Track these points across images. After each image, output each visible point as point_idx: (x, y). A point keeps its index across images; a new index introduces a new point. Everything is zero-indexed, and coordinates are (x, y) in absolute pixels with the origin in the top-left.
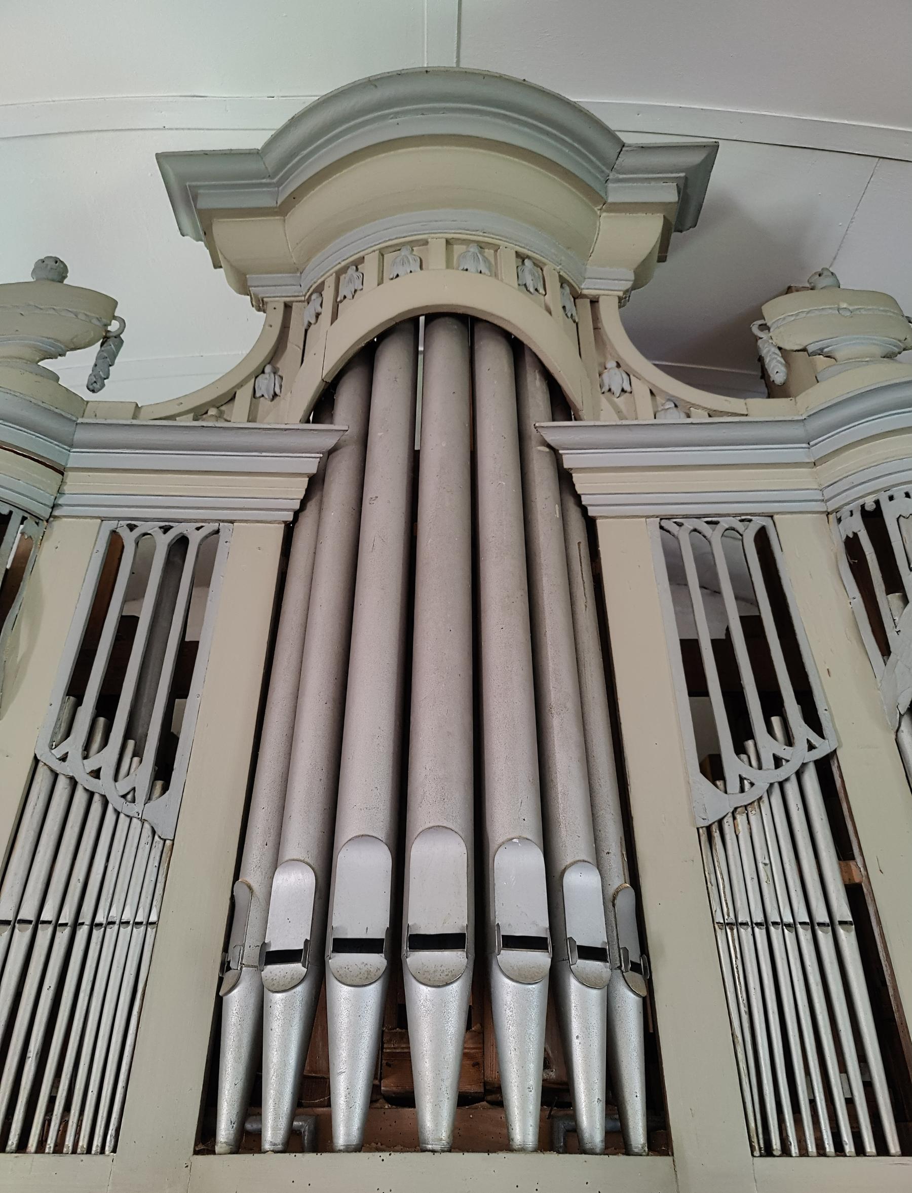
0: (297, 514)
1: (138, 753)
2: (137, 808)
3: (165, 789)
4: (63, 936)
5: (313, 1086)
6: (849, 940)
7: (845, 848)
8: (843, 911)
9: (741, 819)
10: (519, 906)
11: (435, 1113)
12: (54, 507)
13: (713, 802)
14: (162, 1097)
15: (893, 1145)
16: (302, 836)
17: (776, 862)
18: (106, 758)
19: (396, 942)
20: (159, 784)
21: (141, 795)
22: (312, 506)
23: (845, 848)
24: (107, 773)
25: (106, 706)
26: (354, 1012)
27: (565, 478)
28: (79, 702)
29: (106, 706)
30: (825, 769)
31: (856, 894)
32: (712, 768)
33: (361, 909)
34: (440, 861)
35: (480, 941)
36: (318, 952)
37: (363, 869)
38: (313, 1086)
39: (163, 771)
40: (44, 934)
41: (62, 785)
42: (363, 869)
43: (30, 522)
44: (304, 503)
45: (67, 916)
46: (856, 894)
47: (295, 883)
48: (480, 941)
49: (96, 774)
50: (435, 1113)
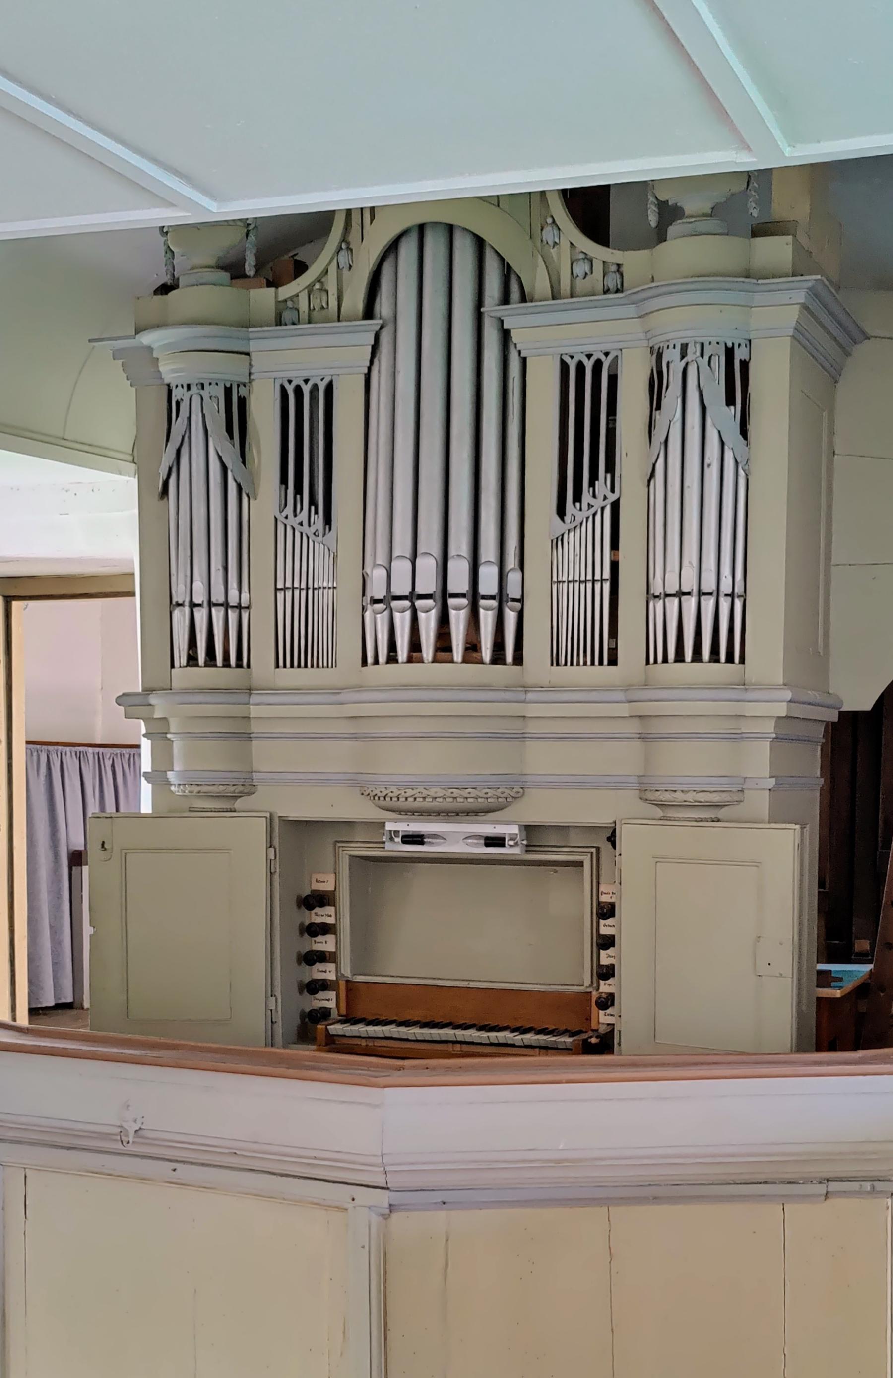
0: (369, 369)
1: (316, 512)
2: (320, 539)
3: (330, 529)
4: (303, 593)
6: (607, 586)
7: (615, 545)
8: (607, 574)
9: (572, 534)
12: (250, 374)
13: (560, 527)
15: (605, 662)
18: (303, 516)
20: (327, 527)
21: (321, 533)
22: (376, 361)
23: (615, 545)
24: (305, 523)
25: (298, 490)
28: (287, 488)
29: (298, 490)
30: (615, 507)
31: (615, 566)
32: (561, 512)
39: (328, 520)
40: (297, 592)
41: (289, 528)
43: (242, 386)
44: (372, 362)
45: (303, 585)
46: (615, 566)
49: (301, 524)
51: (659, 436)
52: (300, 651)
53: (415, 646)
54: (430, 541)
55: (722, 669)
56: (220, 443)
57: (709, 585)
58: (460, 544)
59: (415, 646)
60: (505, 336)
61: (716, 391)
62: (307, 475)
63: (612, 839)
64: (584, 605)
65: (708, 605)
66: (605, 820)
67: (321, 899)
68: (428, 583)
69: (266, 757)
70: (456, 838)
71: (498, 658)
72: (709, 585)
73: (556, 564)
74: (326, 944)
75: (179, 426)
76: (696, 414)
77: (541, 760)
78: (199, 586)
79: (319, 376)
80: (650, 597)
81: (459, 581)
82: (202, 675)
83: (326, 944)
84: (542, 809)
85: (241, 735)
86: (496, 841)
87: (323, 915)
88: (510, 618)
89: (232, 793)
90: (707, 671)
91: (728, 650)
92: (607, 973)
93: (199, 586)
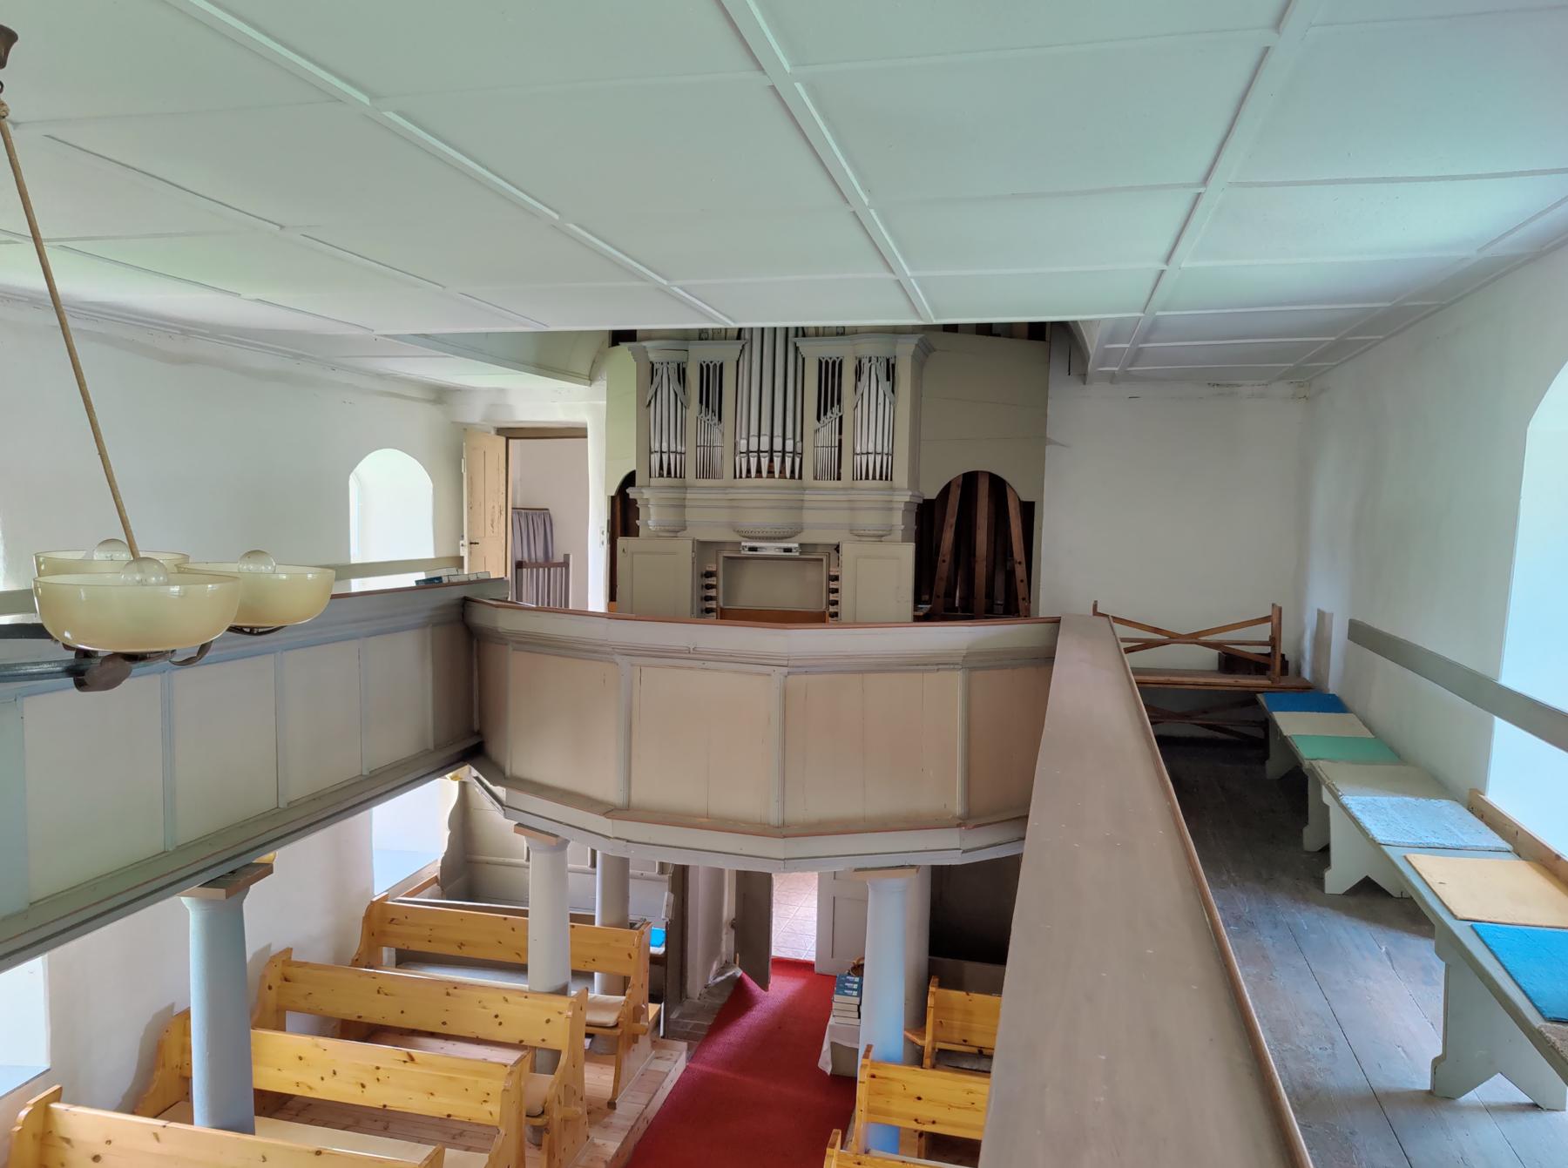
5: (749, 471)
10: (778, 445)
11: (764, 473)
13: (818, 425)
14: (728, 472)
16: (744, 435)
17: (826, 434)
19: (759, 451)
26: (754, 461)
27: (797, 349)
32: (819, 419)
33: (754, 447)
34: (765, 440)
35: (771, 451)
36: (748, 452)
37: (754, 441)
38: (749, 471)
42: (754, 441)
47: (744, 442)
48: (771, 451)
50: (764, 473)
51: (859, 392)
52: (707, 470)
53: (759, 471)
54: (766, 429)
55: (883, 483)
56: (674, 385)
57: (879, 450)
58: (778, 431)
59: (759, 471)
60: (797, 349)
61: (883, 376)
62: (711, 398)
63: (837, 549)
64: (825, 455)
65: (879, 458)
66: (835, 541)
67: (709, 575)
68: (765, 446)
69: (691, 515)
70: (771, 549)
71: (792, 476)
72: (879, 450)
73: (818, 439)
74: (712, 593)
75: (657, 379)
76: (874, 385)
77: (809, 517)
78: (665, 445)
79: (717, 360)
80: (855, 454)
81: (778, 445)
82: (665, 481)
83: (712, 593)
84: (808, 537)
85: (681, 506)
86: (788, 550)
87: (712, 581)
88: (797, 460)
89: (677, 530)
90: (877, 483)
91: (886, 476)
92: (835, 603)
93: (665, 445)
